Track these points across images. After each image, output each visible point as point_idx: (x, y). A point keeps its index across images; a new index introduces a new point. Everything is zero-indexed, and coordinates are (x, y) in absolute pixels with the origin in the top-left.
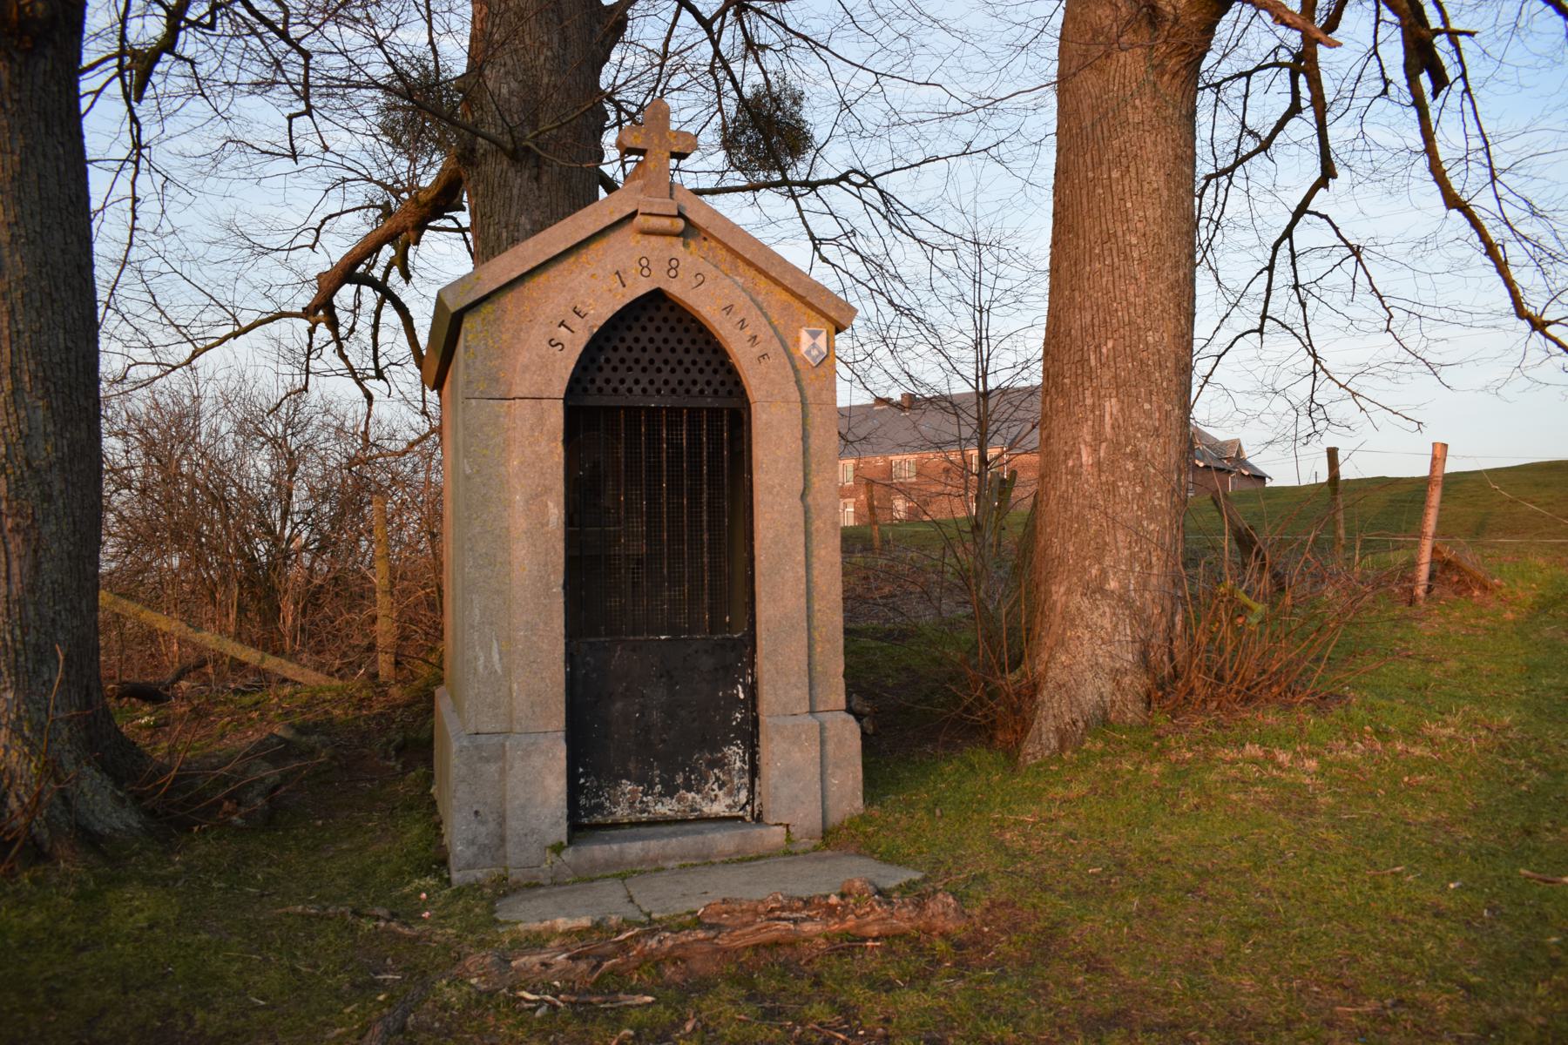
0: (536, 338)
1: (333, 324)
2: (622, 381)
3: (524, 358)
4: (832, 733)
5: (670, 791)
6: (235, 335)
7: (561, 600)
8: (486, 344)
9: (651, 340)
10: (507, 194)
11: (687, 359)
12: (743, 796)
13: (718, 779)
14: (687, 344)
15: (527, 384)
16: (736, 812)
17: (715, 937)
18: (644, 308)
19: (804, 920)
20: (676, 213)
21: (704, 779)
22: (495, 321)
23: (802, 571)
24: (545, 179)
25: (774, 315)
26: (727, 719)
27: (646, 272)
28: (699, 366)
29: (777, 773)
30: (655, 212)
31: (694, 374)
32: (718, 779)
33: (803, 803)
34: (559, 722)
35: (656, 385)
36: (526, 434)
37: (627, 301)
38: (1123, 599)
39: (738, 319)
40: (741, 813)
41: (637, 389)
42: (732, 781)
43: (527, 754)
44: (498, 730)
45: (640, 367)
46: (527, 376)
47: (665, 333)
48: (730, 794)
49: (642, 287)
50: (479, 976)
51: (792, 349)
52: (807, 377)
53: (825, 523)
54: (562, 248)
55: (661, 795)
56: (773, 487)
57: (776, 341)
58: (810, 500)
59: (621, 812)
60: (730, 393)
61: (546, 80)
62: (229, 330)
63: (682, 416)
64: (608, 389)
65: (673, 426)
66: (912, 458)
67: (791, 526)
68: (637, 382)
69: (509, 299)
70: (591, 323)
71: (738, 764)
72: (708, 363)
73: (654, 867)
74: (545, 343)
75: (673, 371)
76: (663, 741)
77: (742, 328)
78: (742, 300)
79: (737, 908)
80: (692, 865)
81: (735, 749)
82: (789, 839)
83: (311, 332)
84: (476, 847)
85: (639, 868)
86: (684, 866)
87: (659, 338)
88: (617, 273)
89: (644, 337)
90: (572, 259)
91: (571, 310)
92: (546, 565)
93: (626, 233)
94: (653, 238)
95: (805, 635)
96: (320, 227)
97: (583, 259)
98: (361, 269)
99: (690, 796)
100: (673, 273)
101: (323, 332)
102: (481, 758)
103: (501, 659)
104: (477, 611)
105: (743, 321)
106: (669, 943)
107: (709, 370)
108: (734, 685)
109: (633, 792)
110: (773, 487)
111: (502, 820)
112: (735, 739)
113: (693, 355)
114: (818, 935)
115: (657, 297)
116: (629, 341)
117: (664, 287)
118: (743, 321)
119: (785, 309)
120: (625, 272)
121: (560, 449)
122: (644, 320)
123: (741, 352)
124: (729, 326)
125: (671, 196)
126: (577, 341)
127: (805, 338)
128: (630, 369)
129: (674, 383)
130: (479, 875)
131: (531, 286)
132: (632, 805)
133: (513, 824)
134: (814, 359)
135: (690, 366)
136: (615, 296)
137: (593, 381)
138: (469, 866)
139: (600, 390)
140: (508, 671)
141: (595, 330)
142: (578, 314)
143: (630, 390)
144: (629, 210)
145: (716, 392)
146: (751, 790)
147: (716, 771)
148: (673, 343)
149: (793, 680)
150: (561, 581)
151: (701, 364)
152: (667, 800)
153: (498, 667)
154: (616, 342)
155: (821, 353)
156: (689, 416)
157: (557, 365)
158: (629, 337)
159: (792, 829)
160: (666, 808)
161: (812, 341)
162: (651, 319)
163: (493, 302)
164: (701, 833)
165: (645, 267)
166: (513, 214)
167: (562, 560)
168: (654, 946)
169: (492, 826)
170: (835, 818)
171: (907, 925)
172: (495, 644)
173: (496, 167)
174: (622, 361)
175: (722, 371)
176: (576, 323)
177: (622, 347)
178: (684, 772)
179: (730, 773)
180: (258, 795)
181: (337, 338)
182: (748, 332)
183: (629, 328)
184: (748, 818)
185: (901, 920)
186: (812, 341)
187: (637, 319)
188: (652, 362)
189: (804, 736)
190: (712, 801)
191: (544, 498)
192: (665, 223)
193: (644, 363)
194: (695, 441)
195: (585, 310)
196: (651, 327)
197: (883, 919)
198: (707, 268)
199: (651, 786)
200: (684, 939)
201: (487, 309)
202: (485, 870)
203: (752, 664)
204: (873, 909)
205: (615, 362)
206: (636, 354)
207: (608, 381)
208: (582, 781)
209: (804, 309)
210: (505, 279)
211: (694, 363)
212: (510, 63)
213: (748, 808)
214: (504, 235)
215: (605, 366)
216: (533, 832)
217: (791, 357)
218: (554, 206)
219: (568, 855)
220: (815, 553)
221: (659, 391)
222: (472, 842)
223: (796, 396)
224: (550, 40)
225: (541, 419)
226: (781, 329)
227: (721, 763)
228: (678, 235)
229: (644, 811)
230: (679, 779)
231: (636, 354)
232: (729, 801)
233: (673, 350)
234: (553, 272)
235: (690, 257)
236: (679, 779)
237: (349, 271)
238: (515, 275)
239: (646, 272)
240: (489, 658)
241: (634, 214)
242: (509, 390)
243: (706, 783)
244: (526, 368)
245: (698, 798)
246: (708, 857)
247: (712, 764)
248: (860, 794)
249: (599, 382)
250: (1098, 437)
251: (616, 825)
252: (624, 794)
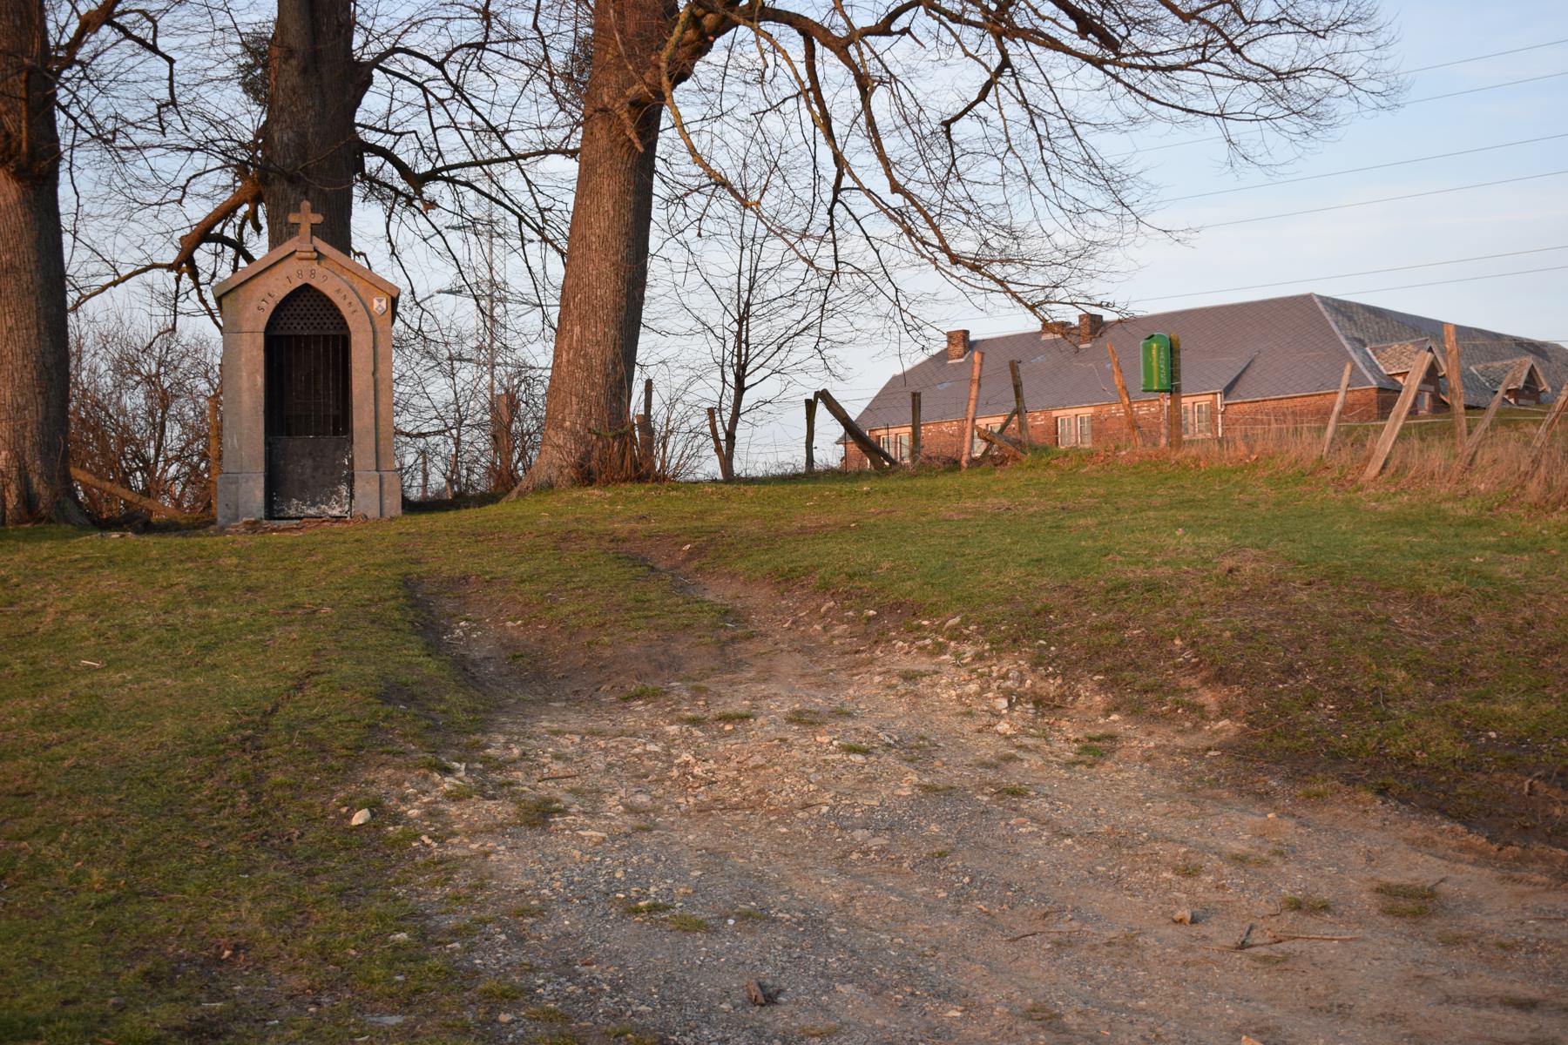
0: (252, 307)
1: (194, 274)
3: (247, 315)
5: (314, 504)
6: (115, 284)
11: (321, 313)
12: (347, 507)
21: (330, 499)
23: (372, 407)
25: (361, 292)
26: (341, 473)
34: (261, 468)
38: (573, 433)
47: (312, 302)
49: (299, 283)
52: (376, 320)
58: (378, 375)
59: (292, 512)
62: (110, 279)
66: (1086, 412)
69: (241, 291)
78: (345, 287)
83: (178, 280)
87: (308, 305)
89: (302, 305)
93: (292, 260)
98: (217, 229)
101: (186, 281)
111: (237, 508)
115: (306, 288)
121: (262, 354)
123: (345, 310)
126: (270, 307)
127: (376, 303)
133: (241, 509)
140: (240, 448)
160: (312, 511)
165: (300, 274)
173: (279, 187)
176: (270, 299)
181: (197, 285)
182: (347, 301)
192: (309, 255)
201: (232, 295)
203: (351, 449)
217: (368, 312)
222: (224, 517)
223: (370, 328)
227: (338, 493)
235: (318, 269)
237: (204, 233)
247: (333, 493)
250: (570, 346)
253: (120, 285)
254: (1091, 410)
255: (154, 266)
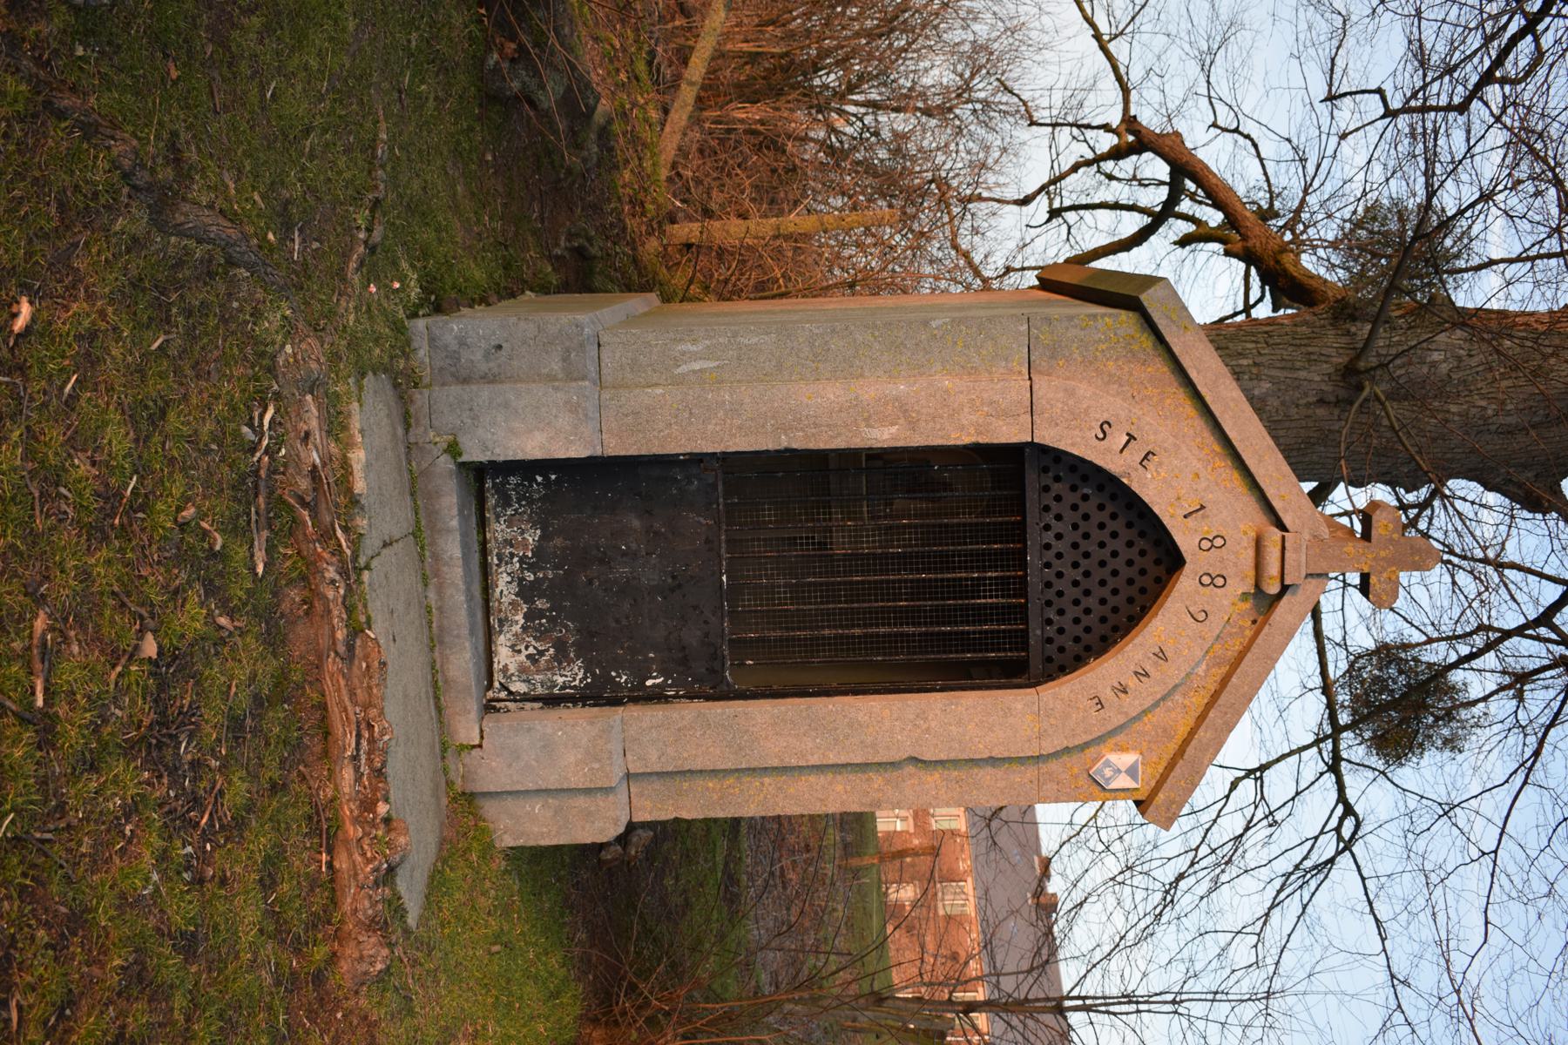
0: (1112, 405)
1: (1117, 154)
2: (1059, 517)
3: (1083, 389)
4: (601, 803)
5: (526, 592)
6: (1097, 36)
7: (771, 446)
8: (1100, 340)
9: (1114, 554)
10: (1298, 364)
11: (1091, 602)
12: (518, 687)
13: (541, 653)
14: (1113, 601)
15: (1050, 395)
16: (498, 678)
17: (337, 653)
18: (1157, 543)
19: (357, 769)
20: (1287, 582)
22: (1131, 351)
23: (814, 760)
24: (1321, 412)
26: (618, 665)
27: (1205, 544)
28: (1081, 523)
29: (549, 731)
30: (1287, 555)
31: (1073, 612)
32: (541, 653)
33: (510, 766)
34: (615, 447)
35: (1055, 562)
36: (985, 395)
37: (1166, 521)
39: (1148, 668)
40: (496, 684)
41: (1049, 537)
42: (538, 672)
43: (574, 409)
44: (604, 371)
45: (1080, 540)
46: (1061, 395)
47: (1126, 572)
48: (522, 670)
49: (1185, 540)
50: (295, 355)
51: (1111, 742)
52: (1075, 763)
53: (878, 790)
54: (1231, 434)
55: (521, 580)
56: (925, 719)
57: (1122, 720)
58: (910, 769)
59: (499, 530)
60: (1049, 660)
61: (1454, 408)
62: (1104, 28)
63: (1015, 596)
64: (1048, 499)
65: (1003, 586)
66: (971, 910)
67: (874, 745)
68: (1059, 537)
69: (1160, 368)
70: (1133, 474)
71: (560, 680)
72: (1088, 630)
73: (428, 573)
74: (1105, 417)
75: (1076, 583)
76: (590, 582)
77: (1136, 673)
78: (1173, 673)
79: (374, 681)
80: (430, 623)
81: (580, 675)
82: (463, 748)
83: (1106, 127)
84: (456, 348)
85: (427, 554)
86: (429, 612)
88: (1202, 507)
90: (1217, 448)
91: (1149, 448)
92: (816, 425)
93: (1258, 518)
94: (1251, 553)
95: (730, 766)
96: (1241, 134)
97: (1219, 463)
98: (1190, 185)
99: (520, 618)
100: (1206, 580)
101: (1106, 142)
102: (568, 350)
103: (694, 372)
104: (755, 340)
105: (1147, 675)
106: (331, 594)
107: (1078, 630)
108: (663, 672)
109: (525, 544)
110: (925, 719)
111: (490, 379)
112: (594, 675)
113: (1098, 610)
114: (336, 789)
115: (1173, 561)
116: (1112, 526)
117: (1187, 569)
118: (1147, 675)
119: (1165, 730)
120: (1203, 517)
121: (966, 440)
122: (1141, 544)
124: (1138, 656)
125: (1309, 575)
126: (1109, 457)
127: (1129, 759)
128: (1075, 527)
129: (1059, 585)
130: (421, 353)
131: (1181, 396)
132: (508, 542)
133: (484, 393)
134: (1100, 772)
135: (1081, 511)
136: (1171, 505)
137: (1057, 479)
138: (432, 340)
139: (1046, 489)
140: (679, 381)
141: (1125, 481)
142: (1146, 457)
143: (1047, 528)
144: (1287, 520)
145: (1050, 641)
146: (526, 698)
147: (552, 651)
148: (1112, 583)
149: (670, 751)
150: (795, 446)
151: (1086, 621)
152: (514, 588)
153: (684, 369)
154: (1110, 509)
155: (1108, 780)
156: (1015, 606)
157: (1077, 432)
158: (1117, 525)
159: (475, 752)
160: (504, 586)
161: (1123, 769)
162: (1142, 553)
163: (1155, 348)
164: (472, 632)
165: (1212, 543)
166: (1274, 372)
167: (822, 446)
168: (326, 575)
169: (483, 367)
170: (490, 809)
171: (347, 908)
172: (712, 364)
173: (1333, 348)
174: (1086, 517)
175: (1078, 649)
176: (1135, 454)
177: (1103, 516)
178: (550, 610)
179: (548, 669)
180: (524, 83)
181: (1099, 159)
182: (1132, 683)
183: (1129, 525)
184: (490, 694)
185: (354, 899)
186: (1123, 769)
187: (1142, 534)
188: (1086, 555)
189: (596, 766)
190: (512, 647)
191: (902, 421)
192: (1273, 568)
193: (1085, 546)
194: (981, 615)
195: (1150, 465)
196: (1133, 553)
197: (356, 874)
198: (1215, 625)
199: (532, 568)
200: (336, 613)
201: (1147, 341)
202: (427, 360)
203: (691, 697)
204: (369, 861)
205: (1084, 507)
206: (1097, 535)
207: (1058, 498)
208: (539, 479)
209: (1167, 757)
210: (1186, 362)
211: (1087, 611)
212: (1474, 362)
213: (503, 695)
214: (1245, 362)
215: (1078, 494)
216: (475, 418)
217: (1100, 740)
218: (1287, 424)
219: (445, 463)
220: (839, 778)
221: (1048, 565)
222: (462, 343)
223: (1048, 749)
224: (1509, 413)
225: (1005, 414)
226: (1137, 726)
227: (561, 657)
228: (1257, 586)
229: (500, 560)
230: (541, 604)
231: (1097, 535)
232: (512, 669)
233: (1103, 583)
234: (1199, 424)
235: (1229, 601)
236: (541, 604)
238: (1193, 375)
239: (1205, 544)
240: (696, 357)
241: (1281, 526)
242: (1040, 373)
243: (535, 638)
244: (1071, 393)
245: (517, 628)
246: (441, 643)
247: (560, 647)
248: (521, 842)
249: (1057, 488)
251: (482, 524)
252: (522, 533)
253: (1095, 43)
254: (973, 915)
255: (1126, 91)
